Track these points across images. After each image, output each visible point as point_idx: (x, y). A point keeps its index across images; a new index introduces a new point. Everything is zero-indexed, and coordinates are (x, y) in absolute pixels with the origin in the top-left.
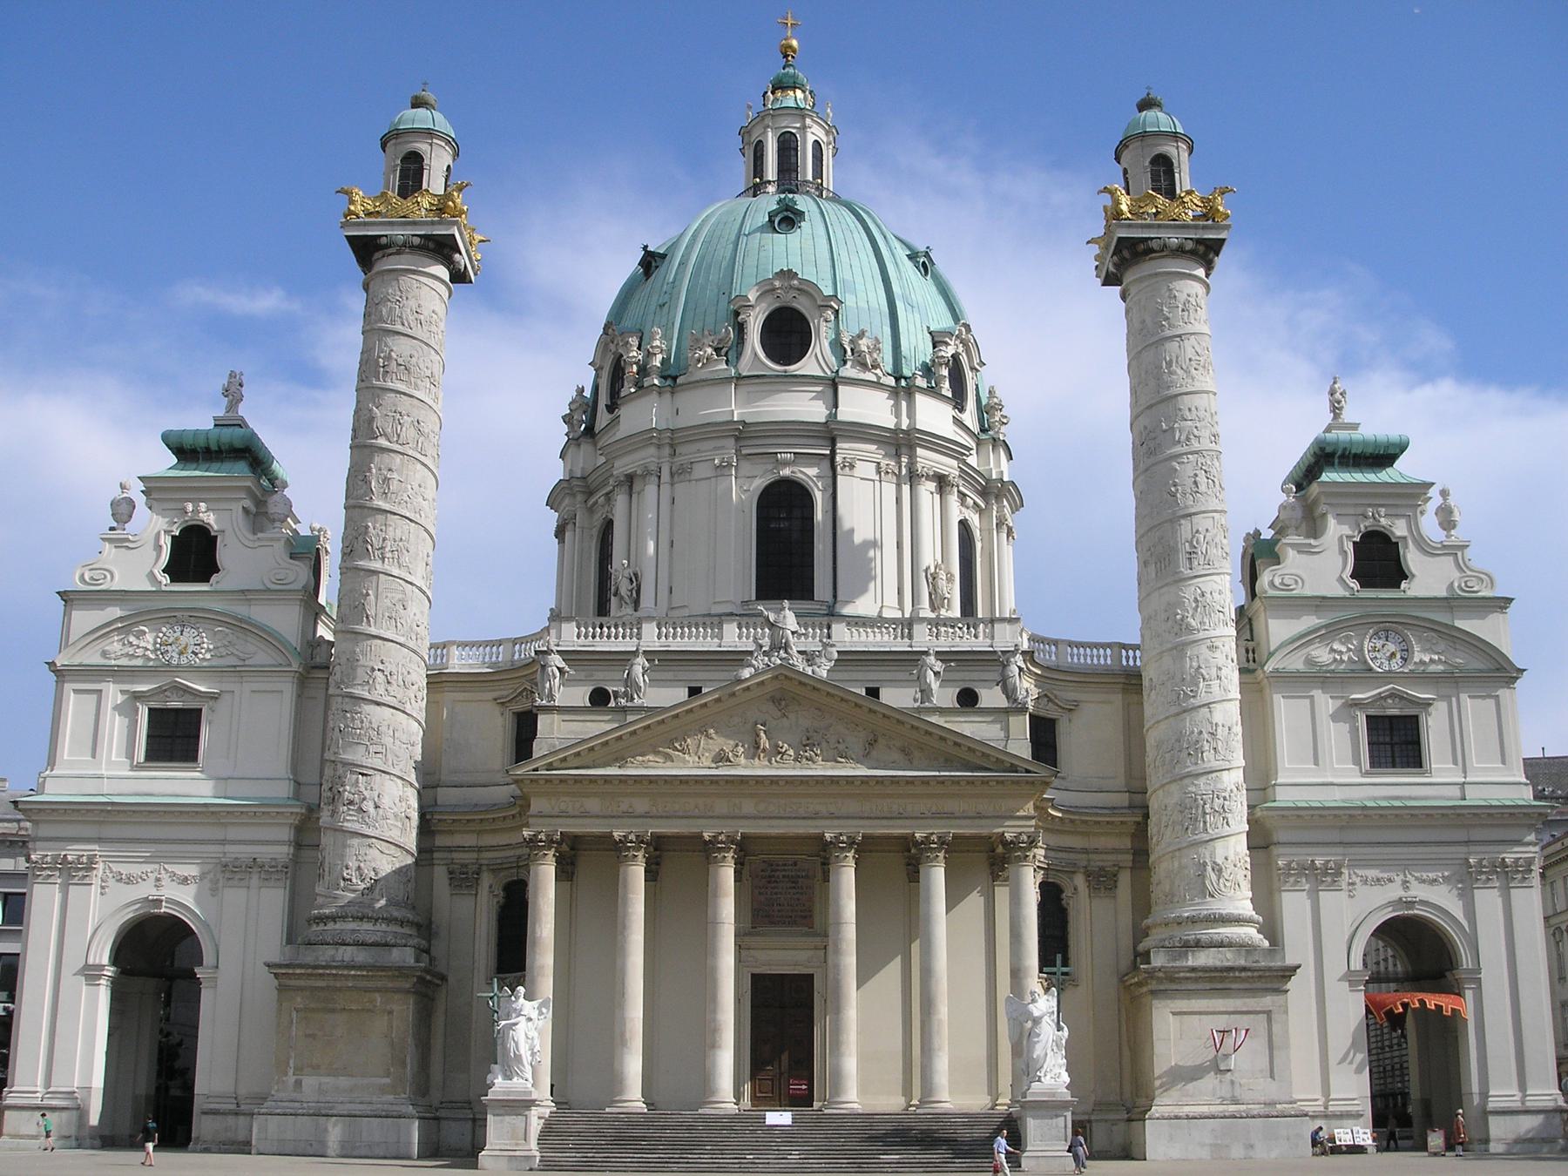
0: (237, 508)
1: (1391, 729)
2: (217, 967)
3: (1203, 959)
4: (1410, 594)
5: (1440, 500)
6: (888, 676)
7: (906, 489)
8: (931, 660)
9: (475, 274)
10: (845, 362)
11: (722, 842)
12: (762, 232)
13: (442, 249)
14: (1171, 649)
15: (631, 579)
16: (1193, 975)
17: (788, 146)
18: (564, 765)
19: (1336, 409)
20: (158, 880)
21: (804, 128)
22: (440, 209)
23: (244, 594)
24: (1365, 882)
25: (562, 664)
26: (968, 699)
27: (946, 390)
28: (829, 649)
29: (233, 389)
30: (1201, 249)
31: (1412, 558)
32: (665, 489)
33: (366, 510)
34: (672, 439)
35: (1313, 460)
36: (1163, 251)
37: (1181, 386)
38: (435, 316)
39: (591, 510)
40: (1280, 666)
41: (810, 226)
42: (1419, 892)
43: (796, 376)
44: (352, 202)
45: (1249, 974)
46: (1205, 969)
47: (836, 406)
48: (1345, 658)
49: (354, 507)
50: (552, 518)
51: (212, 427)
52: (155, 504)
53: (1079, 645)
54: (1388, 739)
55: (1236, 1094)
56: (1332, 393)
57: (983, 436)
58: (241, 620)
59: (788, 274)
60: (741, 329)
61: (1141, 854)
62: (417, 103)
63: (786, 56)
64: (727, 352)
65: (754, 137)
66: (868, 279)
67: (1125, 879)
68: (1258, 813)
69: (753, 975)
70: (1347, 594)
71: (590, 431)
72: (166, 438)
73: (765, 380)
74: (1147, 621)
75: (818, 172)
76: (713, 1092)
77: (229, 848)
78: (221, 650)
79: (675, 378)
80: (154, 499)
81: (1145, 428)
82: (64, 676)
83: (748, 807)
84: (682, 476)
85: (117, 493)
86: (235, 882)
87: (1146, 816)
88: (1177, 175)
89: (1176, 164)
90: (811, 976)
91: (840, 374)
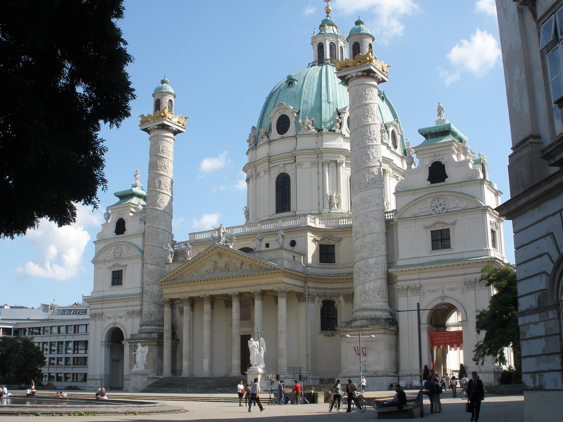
1: (441, 235)
3: (358, 323)
4: (449, 183)
6: (271, 239)
7: (321, 168)
9: (185, 129)
16: (352, 330)
17: (321, 47)
19: (439, 114)
20: (115, 318)
24: (429, 291)
30: (365, 73)
32: (254, 181)
37: (358, 125)
38: (165, 148)
42: (447, 293)
43: (284, 138)
45: (369, 328)
46: (357, 327)
54: (440, 238)
55: (368, 369)
56: (438, 109)
60: (271, 124)
63: (327, 13)
68: (390, 270)
73: (275, 141)
77: (128, 308)
83: (212, 287)
85: (106, 211)
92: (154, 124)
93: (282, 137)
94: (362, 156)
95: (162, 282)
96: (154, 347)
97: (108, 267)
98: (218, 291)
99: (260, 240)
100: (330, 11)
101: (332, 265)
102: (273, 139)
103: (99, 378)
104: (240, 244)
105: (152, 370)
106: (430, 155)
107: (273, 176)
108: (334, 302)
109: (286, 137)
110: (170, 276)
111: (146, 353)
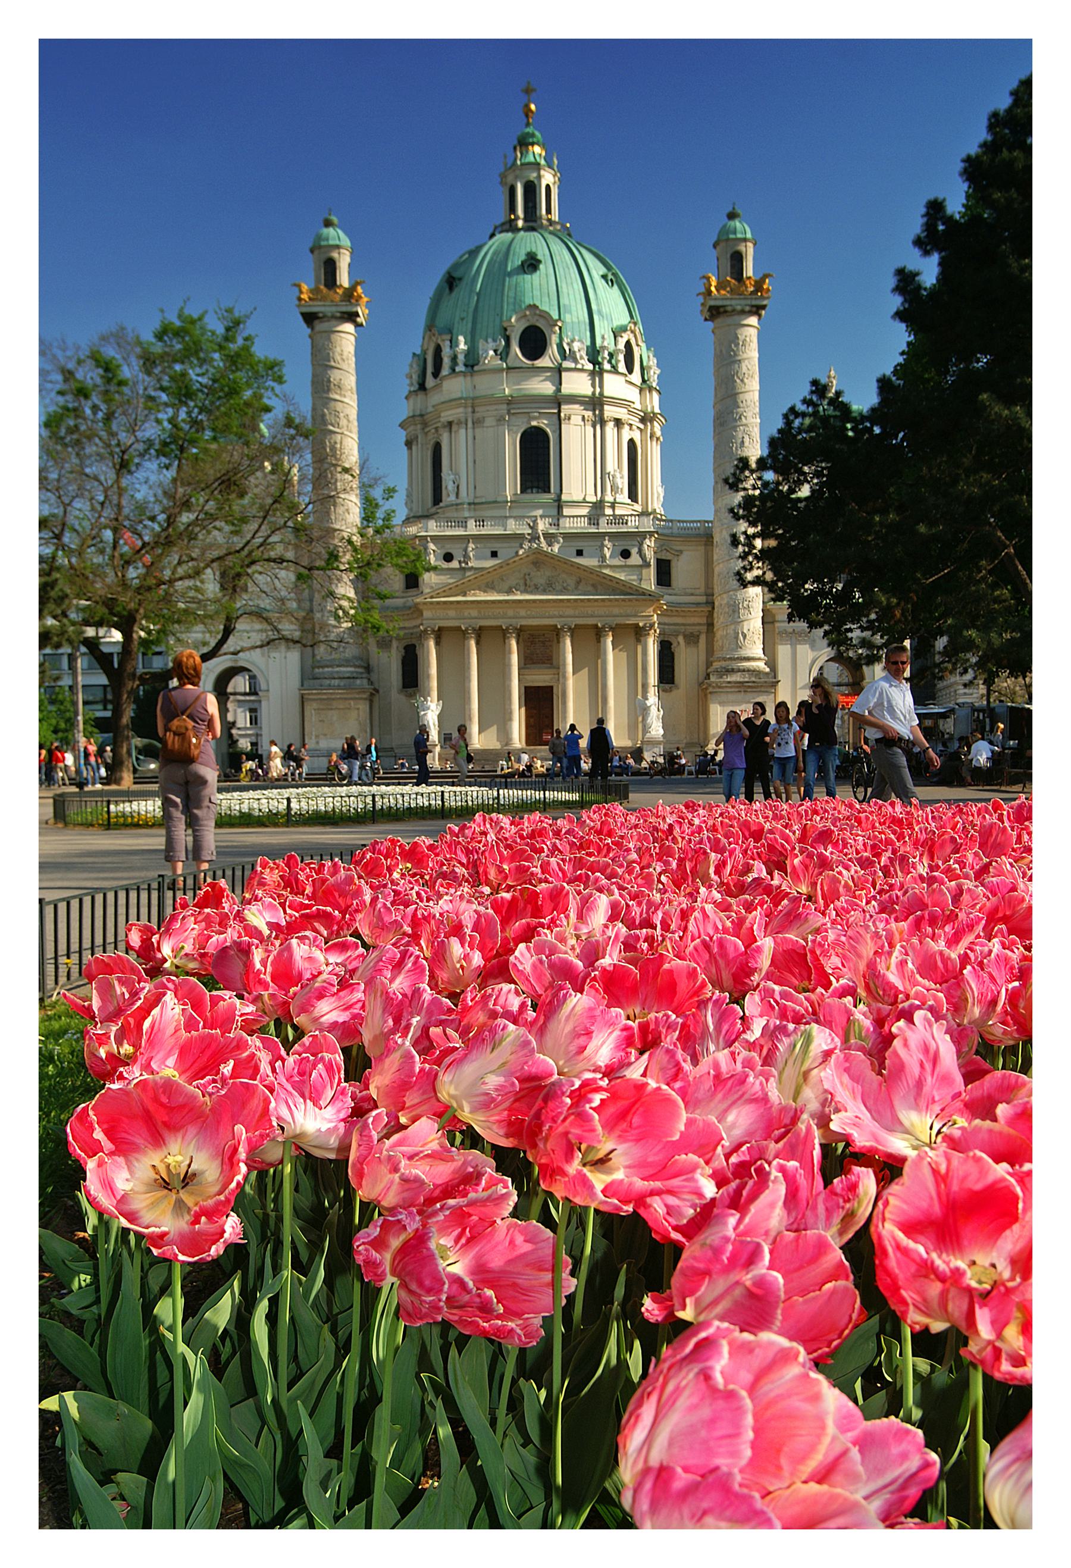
6: (586, 544)
7: (598, 427)
12: (518, 274)
13: (352, 317)
17: (531, 189)
21: (539, 177)
25: (434, 548)
26: (626, 554)
27: (622, 367)
32: (470, 431)
44: (301, 292)
50: (402, 436)
53: (683, 522)
57: (644, 386)
59: (535, 307)
60: (508, 340)
61: (710, 625)
62: (328, 224)
63: (527, 116)
65: (510, 179)
66: (578, 301)
67: (703, 639)
69: (526, 688)
71: (422, 387)
74: (716, 511)
75: (549, 211)
76: (511, 739)
79: (472, 367)
83: (523, 613)
87: (713, 608)
90: (552, 687)
92: (334, 309)
96: (361, 702)
101: (670, 591)
108: (671, 644)
111: (438, 713)
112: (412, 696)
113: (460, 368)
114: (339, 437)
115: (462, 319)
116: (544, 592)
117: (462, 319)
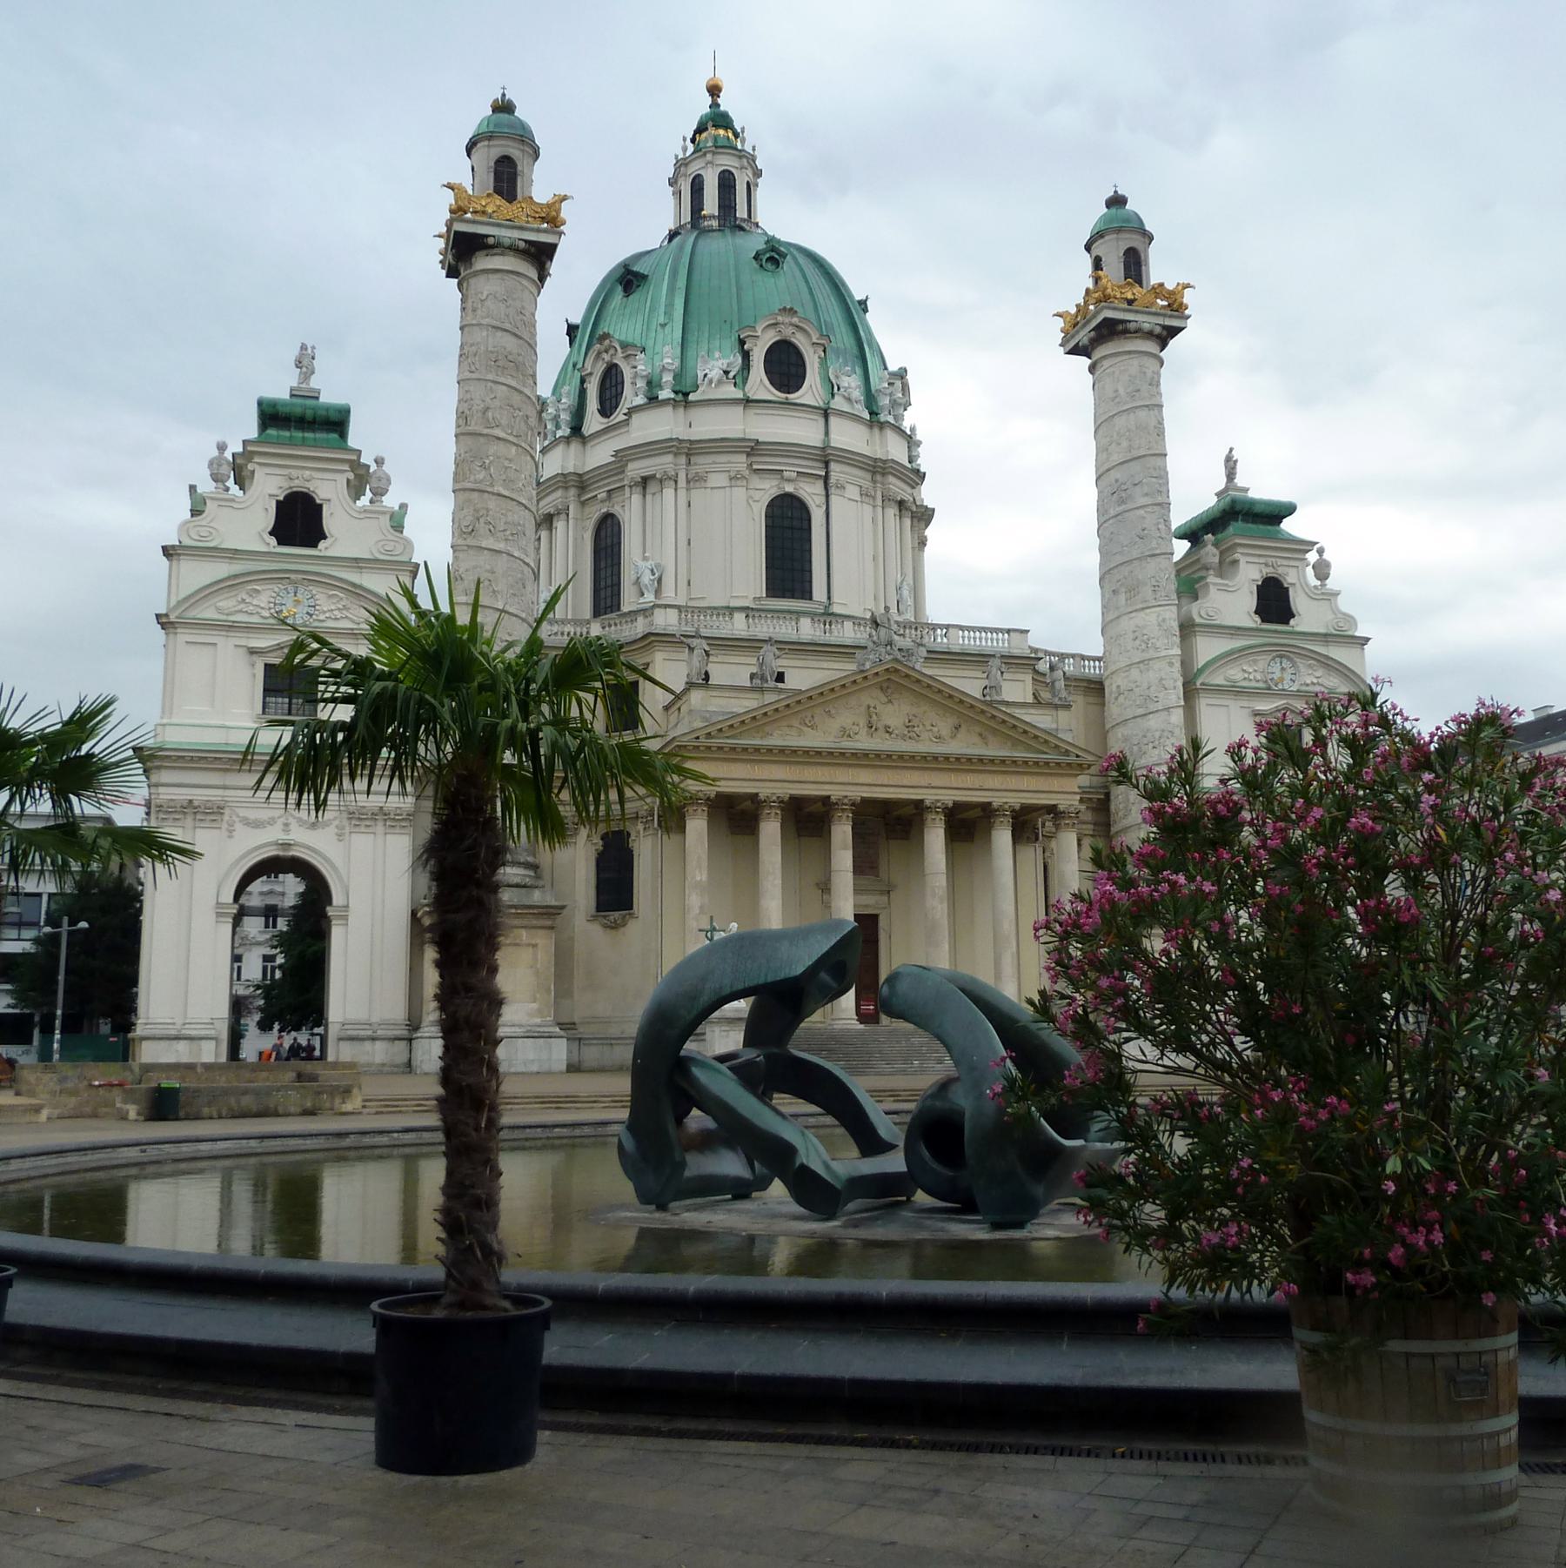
0: (342, 480)
2: (347, 906)
4: (1298, 629)
5: (1317, 557)
8: (997, 662)
10: (833, 395)
11: (843, 804)
14: (1139, 663)
15: (652, 571)
17: (727, 183)
18: (721, 735)
19: (1231, 475)
20: (286, 825)
22: (542, 218)
23: (356, 563)
28: (921, 648)
29: (305, 362)
30: (1165, 333)
31: (1298, 601)
32: (682, 493)
33: (486, 494)
34: (689, 449)
35: (1218, 515)
36: (1136, 332)
39: (583, 504)
40: (1206, 681)
41: (788, 264)
47: (827, 433)
48: (1251, 677)
49: (473, 490)
51: (288, 397)
52: (257, 467)
58: (354, 585)
59: (792, 312)
60: (746, 356)
64: (734, 377)
65: (694, 169)
70: (1254, 625)
71: (576, 430)
72: (260, 403)
78: (336, 613)
79: (686, 395)
80: (260, 464)
81: (1117, 481)
82: (176, 628)
83: (865, 776)
84: (698, 483)
86: (363, 829)
88: (1143, 267)
89: (1143, 258)
91: (832, 406)
92: (516, 234)
93: (787, 398)
94: (1158, 523)
95: (698, 738)
96: (541, 932)
97: (249, 648)
98: (885, 789)
99: (1002, 673)
100: (720, 90)
102: (755, 398)
103: (213, 1032)
104: (836, 666)
105: (535, 1006)
106: (1262, 560)
107: (757, 495)
109: (798, 401)
110: (731, 726)
112: (614, 926)
113: (665, 394)
114: (514, 449)
115: (666, 324)
116: (903, 737)
117: (663, 326)
